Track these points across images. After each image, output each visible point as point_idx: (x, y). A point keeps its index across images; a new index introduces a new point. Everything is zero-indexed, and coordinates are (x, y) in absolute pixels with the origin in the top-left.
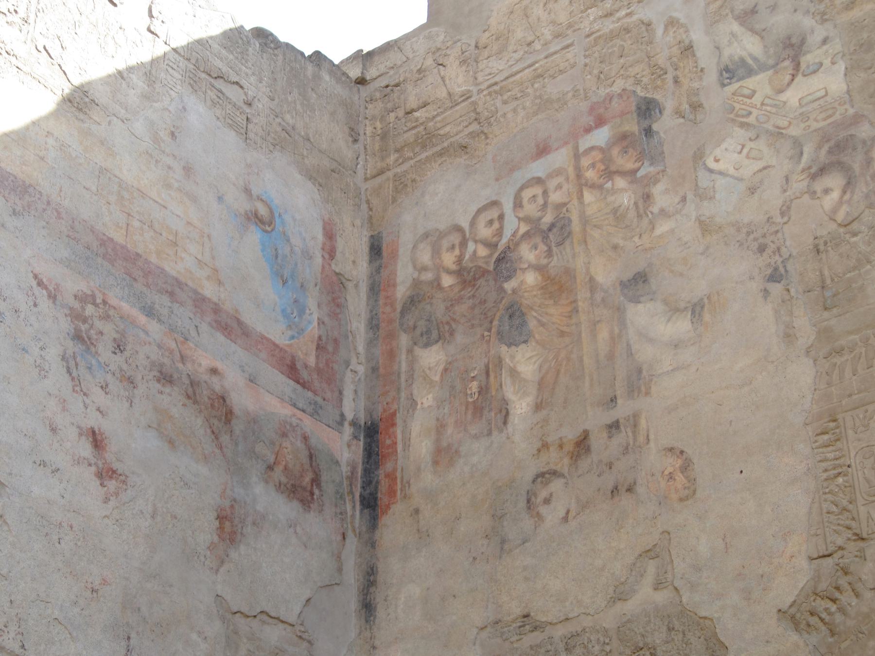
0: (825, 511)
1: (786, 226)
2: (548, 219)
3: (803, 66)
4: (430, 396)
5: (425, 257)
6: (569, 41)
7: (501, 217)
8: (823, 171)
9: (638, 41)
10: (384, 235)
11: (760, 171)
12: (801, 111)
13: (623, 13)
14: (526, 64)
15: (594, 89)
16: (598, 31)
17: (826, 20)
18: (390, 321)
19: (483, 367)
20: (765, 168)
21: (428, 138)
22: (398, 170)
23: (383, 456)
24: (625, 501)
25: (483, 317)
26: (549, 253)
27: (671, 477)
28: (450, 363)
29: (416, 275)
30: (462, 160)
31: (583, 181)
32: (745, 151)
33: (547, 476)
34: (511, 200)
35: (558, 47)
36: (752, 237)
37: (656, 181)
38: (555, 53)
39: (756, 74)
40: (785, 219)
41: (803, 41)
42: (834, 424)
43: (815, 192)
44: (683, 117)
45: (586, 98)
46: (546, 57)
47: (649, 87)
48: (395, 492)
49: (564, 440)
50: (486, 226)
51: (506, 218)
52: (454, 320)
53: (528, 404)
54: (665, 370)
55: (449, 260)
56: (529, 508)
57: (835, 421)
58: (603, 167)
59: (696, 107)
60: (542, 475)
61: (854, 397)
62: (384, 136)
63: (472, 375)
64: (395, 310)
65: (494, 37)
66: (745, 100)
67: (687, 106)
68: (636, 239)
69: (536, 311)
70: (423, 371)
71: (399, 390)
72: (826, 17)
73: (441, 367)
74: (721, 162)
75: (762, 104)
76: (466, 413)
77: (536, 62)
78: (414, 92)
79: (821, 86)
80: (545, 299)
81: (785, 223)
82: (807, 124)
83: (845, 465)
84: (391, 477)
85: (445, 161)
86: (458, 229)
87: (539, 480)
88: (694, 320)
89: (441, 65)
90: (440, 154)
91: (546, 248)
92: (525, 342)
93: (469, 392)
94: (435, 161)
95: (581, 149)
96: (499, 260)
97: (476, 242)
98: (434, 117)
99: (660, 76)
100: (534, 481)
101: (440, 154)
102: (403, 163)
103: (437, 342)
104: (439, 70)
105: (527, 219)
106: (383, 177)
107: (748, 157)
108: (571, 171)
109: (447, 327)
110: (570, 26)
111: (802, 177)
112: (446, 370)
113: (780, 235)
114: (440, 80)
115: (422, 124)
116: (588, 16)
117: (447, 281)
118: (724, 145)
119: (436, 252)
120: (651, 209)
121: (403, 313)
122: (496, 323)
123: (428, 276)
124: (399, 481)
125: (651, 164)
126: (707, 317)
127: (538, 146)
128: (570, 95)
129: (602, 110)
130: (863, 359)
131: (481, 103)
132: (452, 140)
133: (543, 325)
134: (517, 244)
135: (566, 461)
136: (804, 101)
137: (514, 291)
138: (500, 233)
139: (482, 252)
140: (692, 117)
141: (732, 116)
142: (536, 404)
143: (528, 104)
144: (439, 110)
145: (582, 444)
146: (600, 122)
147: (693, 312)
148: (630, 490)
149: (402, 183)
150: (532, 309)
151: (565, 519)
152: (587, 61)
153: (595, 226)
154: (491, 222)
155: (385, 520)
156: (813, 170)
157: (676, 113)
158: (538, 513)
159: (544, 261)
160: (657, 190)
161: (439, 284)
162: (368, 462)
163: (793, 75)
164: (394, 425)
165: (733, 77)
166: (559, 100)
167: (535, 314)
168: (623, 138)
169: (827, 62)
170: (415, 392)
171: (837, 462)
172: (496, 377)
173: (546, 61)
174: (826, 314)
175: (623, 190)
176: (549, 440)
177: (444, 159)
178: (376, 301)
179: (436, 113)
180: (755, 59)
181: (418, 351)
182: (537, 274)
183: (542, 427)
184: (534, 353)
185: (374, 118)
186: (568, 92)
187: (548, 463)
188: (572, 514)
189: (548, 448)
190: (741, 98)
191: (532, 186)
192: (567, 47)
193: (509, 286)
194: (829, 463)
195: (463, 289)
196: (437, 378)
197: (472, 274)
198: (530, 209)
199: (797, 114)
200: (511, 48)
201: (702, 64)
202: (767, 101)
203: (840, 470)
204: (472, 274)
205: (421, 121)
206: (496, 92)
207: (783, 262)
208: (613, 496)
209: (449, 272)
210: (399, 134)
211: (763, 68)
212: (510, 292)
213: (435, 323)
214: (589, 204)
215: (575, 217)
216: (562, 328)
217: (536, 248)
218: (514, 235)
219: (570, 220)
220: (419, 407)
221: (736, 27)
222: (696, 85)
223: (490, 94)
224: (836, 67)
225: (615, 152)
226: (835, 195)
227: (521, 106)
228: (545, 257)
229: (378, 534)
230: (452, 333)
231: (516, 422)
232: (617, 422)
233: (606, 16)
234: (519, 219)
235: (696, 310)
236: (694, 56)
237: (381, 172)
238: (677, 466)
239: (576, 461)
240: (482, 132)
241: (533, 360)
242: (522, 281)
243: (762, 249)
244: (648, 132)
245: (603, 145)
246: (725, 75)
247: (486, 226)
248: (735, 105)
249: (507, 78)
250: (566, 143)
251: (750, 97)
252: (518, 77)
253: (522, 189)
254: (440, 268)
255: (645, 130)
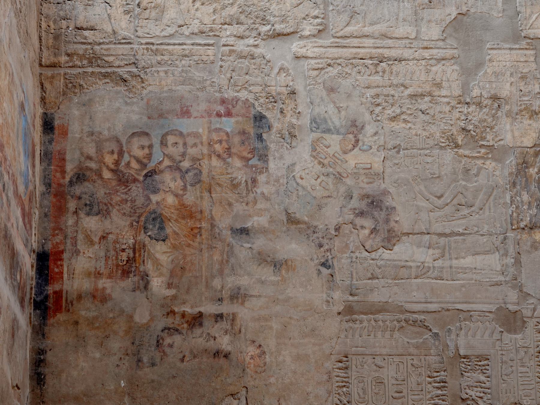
0: (335, 402)
1: (336, 237)
2: (186, 164)
3: (360, 143)
4: (91, 250)
5: (91, 150)
6: (211, 42)
7: (151, 147)
8: (361, 214)
9: (259, 69)
10: (56, 116)
11: (326, 197)
12: (355, 171)
13: (251, 41)
14: (177, 42)
15: (226, 88)
16: (232, 46)
17: (379, 121)
18: (60, 185)
19: (131, 246)
20: (329, 197)
21: (94, 57)
22: (69, 71)
23: (52, 278)
24: (222, 361)
25: (132, 211)
26: (185, 189)
27: (252, 358)
28: (107, 234)
29: (83, 159)
30: (122, 88)
31: (213, 150)
32: (319, 180)
33: (172, 330)
34: (160, 138)
35: (203, 42)
36: (315, 235)
37: (261, 173)
38: (200, 45)
39: (333, 134)
40: (337, 233)
41: (363, 127)
42: (346, 359)
43: (356, 225)
44: (284, 139)
45: (220, 92)
46: (193, 44)
47: (264, 106)
48: (61, 306)
49: (186, 313)
50: (139, 148)
51: (154, 150)
52: (111, 204)
53: (162, 282)
54: (254, 294)
55: (109, 160)
56: (158, 346)
57: (347, 357)
58: (227, 146)
59: (293, 136)
60: (169, 329)
61: (359, 349)
62: (57, 37)
63: (123, 248)
64: (64, 178)
65: (153, 5)
66: (324, 147)
67: (287, 133)
68: (244, 204)
69: (172, 223)
70: (86, 231)
71: (66, 237)
72: (378, 118)
73: (100, 234)
74: (304, 180)
75: (334, 155)
76: (116, 271)
77: (185, 44)
78: (83, 14)
79: (369, 162)
80: (180, 217)
81: (336, 236)
82: (358, 181)
83: (348, 382)
84: (58, 294)
85: (108, 83)
86: (118, 141)
87: (166, 331)
88: (275, 271)
89: (108, 4)
90: (106, 75)
91: (183, 184)
92: (164, 241)
93: (119, 257)
94: (99, 79)
95: (213, 127)
96: (146, 176)
97: (130, 156)
98: (100, 44)
99: (271, 102)
100: (162, 331)
101: (106, 75)
102: (72, 67)
103: (97, 214)
104: (106, 6)
105: (170, 157)
106: (56, 71)
107: (320, 184)
108: (205, 138)
109: (105, 208)
110: (211, 30)
111: (350, 213)
112: (103, 238)
113: (332, 241)
114: (106, 15)
115: (90, 44)
116: (226, 30)
117: (107, 175)
118: (307, 171)
119: (99, 150)
120: (255, 189)
121: (71, 183)
122: (143, 219)
123: (93, 165)
124: (64, 299)
125: (259, 160)
126: (284, 272)
127: (182, 108)
128: (208, 82)
129: (230, 107)
130: (366, 330)
131: (140, 53)
132: (116, 70)
133: (177, 234)
134: (161, 172)
135: (185, 325)
136: (358, 166)
137: (157, 203)
138: (149, 156)
139: (134, 165)
140: (289, 141)
141: (314, 154)
142: (168, 284)
143: (176, 73)
144: (104, 40)
145: (197, 320)
146: (229, 114)
147: (275, 266)
148: (226, 356)
149: (71, 83)
150: (169, 220)
151: (182, 360)
152: (223, 63)
153: (218, 184)
154: (143, 147)
155: (52, 321)
156: (357, 212)
157: (279, 133)
158: (163, 351)
159: (181, 192)
160: (262, 178)
161: (100, 175)
162: (39, 278)
163: (354, 146)
164: (61, 260)
165: (318, 128)
166: (200, 82)
167: (171, 225)
168: (243, 133)
169: (375, 148)
170: (79, 242)
171: (344, 379)
172: (140, 255)
173: (192, 47)
174: (351, 298)
175: (239, 169)
176: (176, 310)
177: (107, 81)
178: (49, 165)
179: (101, 41)
180: (333, 123)
181: (82, 215)
182: (175, 199)
183: (171, 300)
184: (169, 250)
185: (47, 17)
186: (206, 80)
187: (173, 323)
188: (187, 359)
189: (174, 314)
190: (321, 145)
191: (175, 135)
192: (209, 45)
193: (155, 198)
194: (340, 379)
195: (119, 185)
196: (96, 239)
197: (126, 177)
198: (171, 150)
199: (352, 171)
200: (165, 21)
201: (300, 109)
202: (336, 154)
203: (345, 384)
204: (126, 177)
205: (89, 42)
206: (152, 50)
207: (332, 258)
208: (214, 358)
209: (108, 167)
210: (69, 42)
211: (338, 133)
212: (154, 202)
213: (96, 200)
214: (215, 167)
215: (205, 172)
216: (189, 242)
217: (176, 181)
218: (160, 163)
219: (200, 172)
220: (81, 254)
221: (324, 93)
222: (294, 121)
223: (147, 49)
224: (379, 153)
225: (236, 140)
226: (367, 232)
227: (171, 72)
228: (181, 190)
229: (46, 329)
230: (108, 213)
231: (154, 289)
232: (222, 314)
233: (239, 37)
234: (164, 154)
235: (278, 265)
236: (296, 101)
237: (53, 66)
238: (256, 352)
239: (192, 328)
240: (139, 76)
241: (168, 255)
242: (164, 199)
243: (321, 246)
244: (260, 137)
245: (229, 130)
246: (314, 125)
247: (139, 148)
248: (317, 148)
249: (162, 44)
250: (202, 117)
251: (328, 147)
252: (170, 47)
253: (167, 134)
254: (101, 161)
255: (257, 134)
